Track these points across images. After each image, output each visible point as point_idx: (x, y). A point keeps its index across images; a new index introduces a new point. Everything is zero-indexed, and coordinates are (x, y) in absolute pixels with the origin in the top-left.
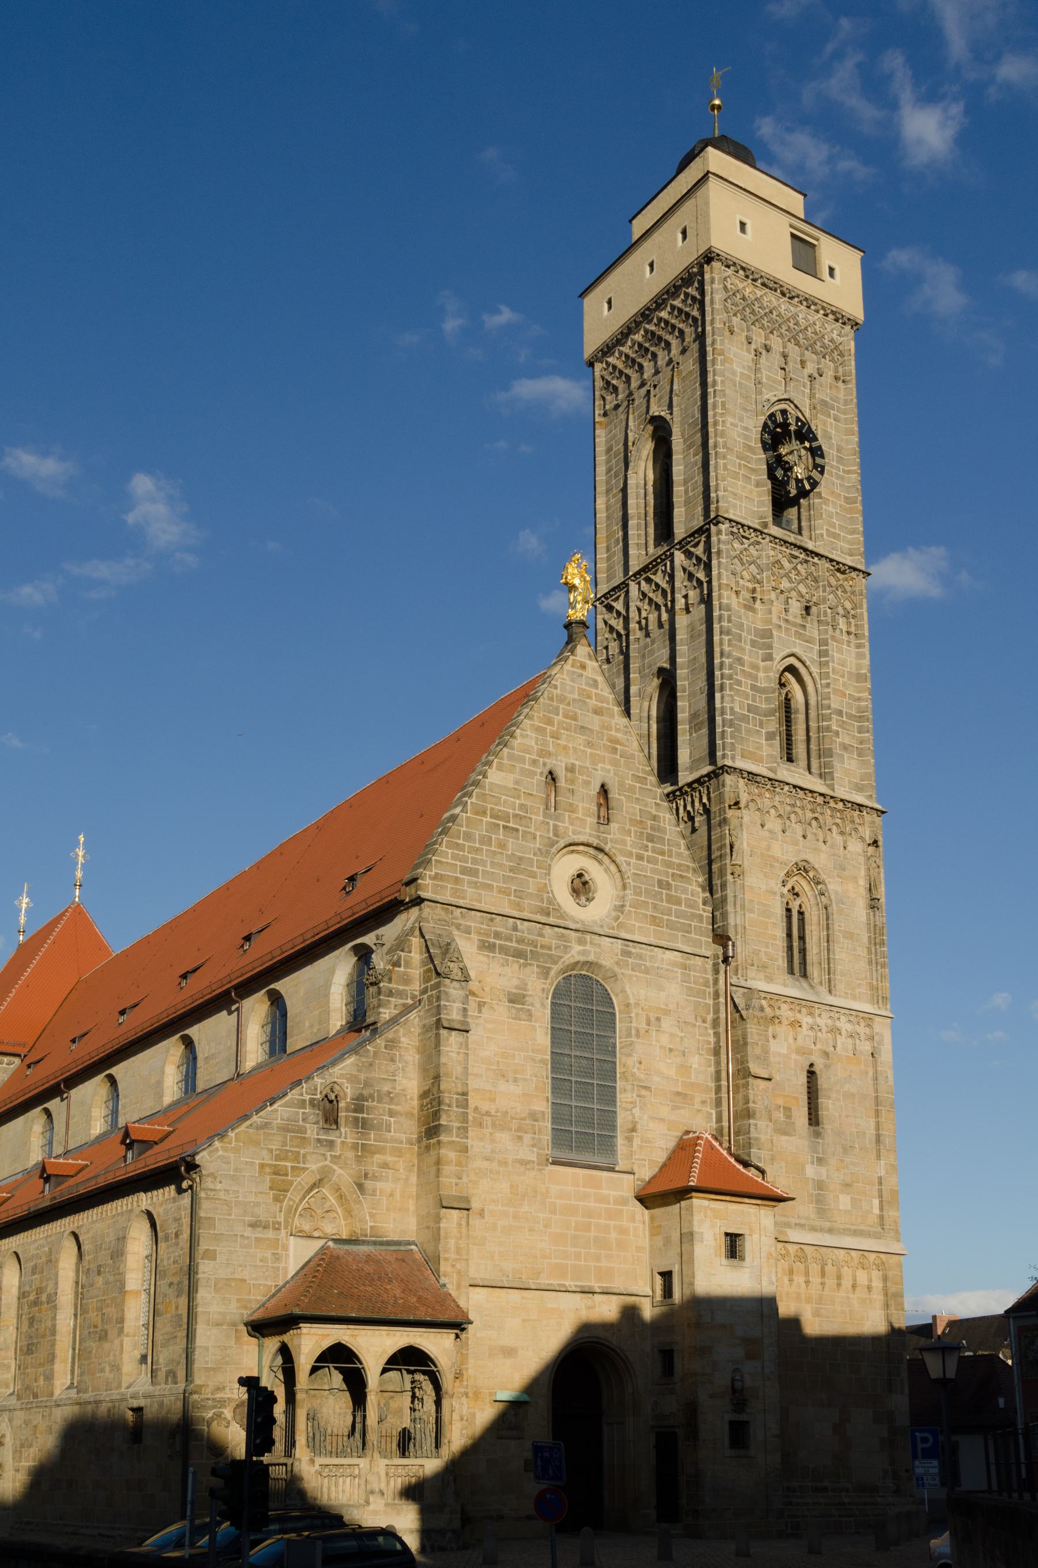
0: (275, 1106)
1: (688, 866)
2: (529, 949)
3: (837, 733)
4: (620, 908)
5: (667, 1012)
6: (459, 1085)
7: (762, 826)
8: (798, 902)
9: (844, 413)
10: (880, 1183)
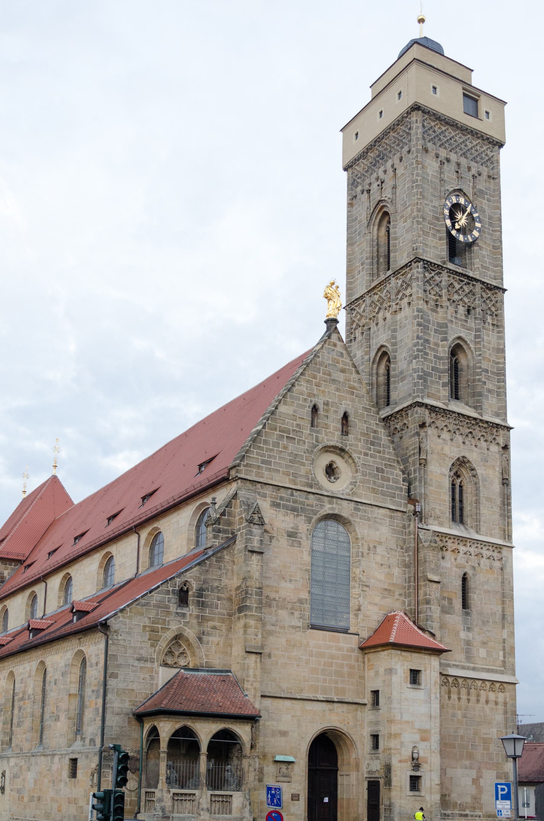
0: (153, 594)
1: (394, 460)
2: (300, 506)
3: (485, 383)
4: (354, 483)
5: (380, 543)
6: (257, 583)
7: (439, 436)
8: (459, 480)
9: (493, 197)
10: (504, 642)
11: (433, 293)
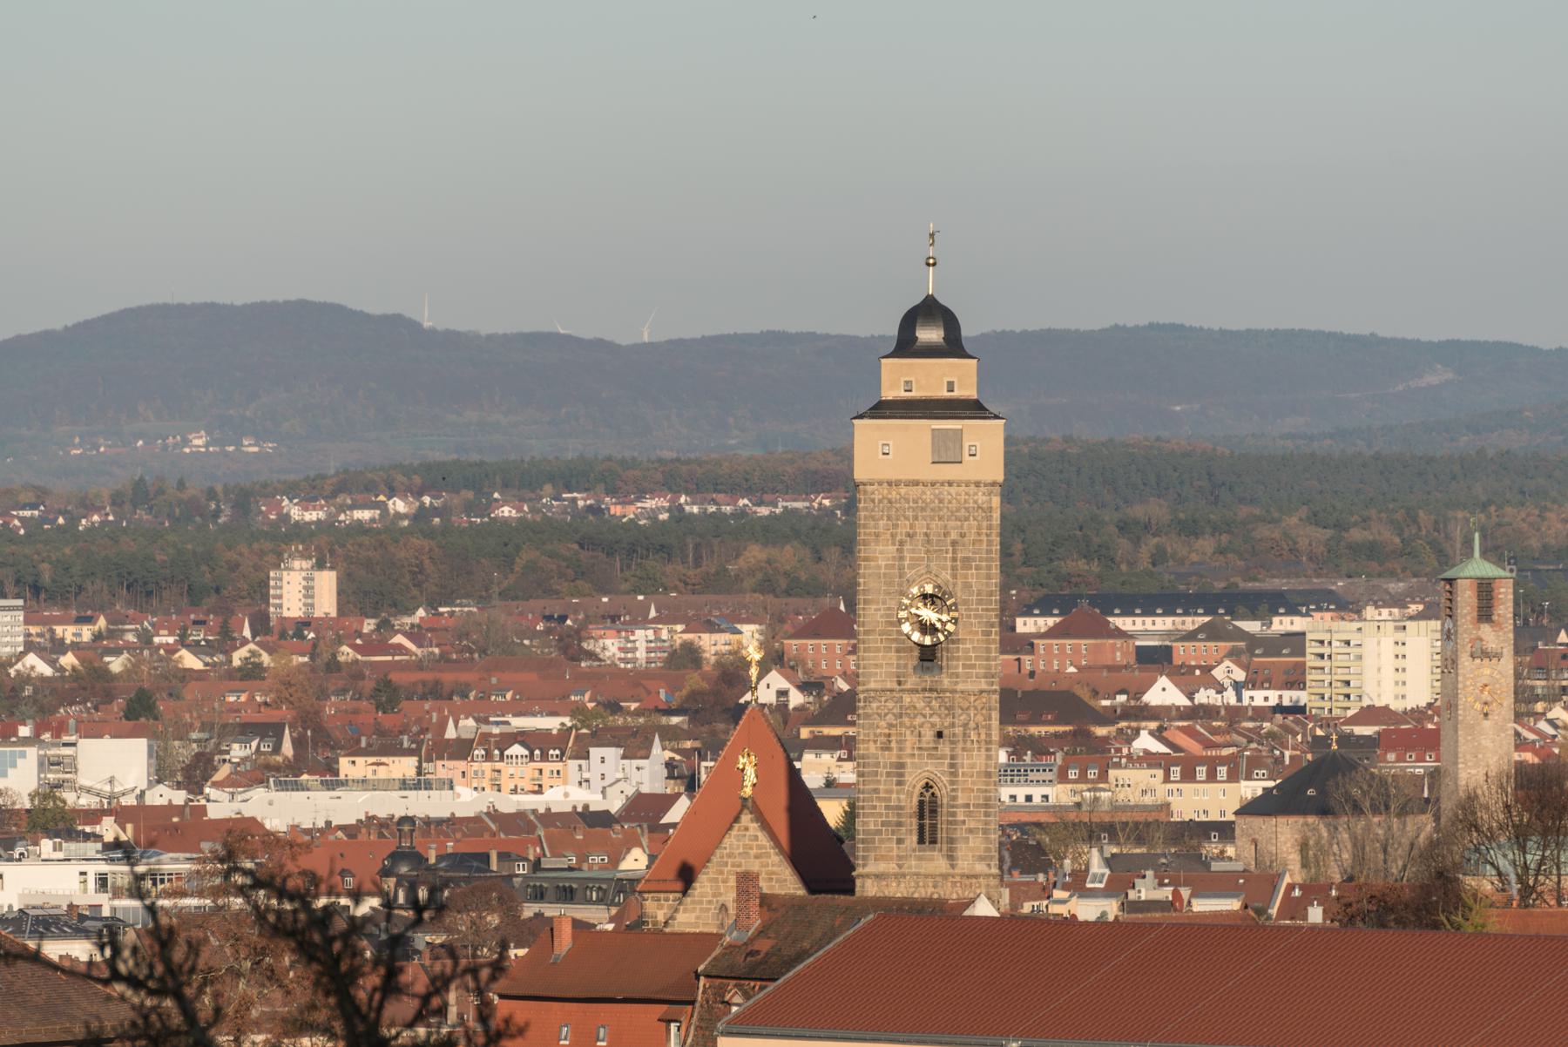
11: (883, 723)
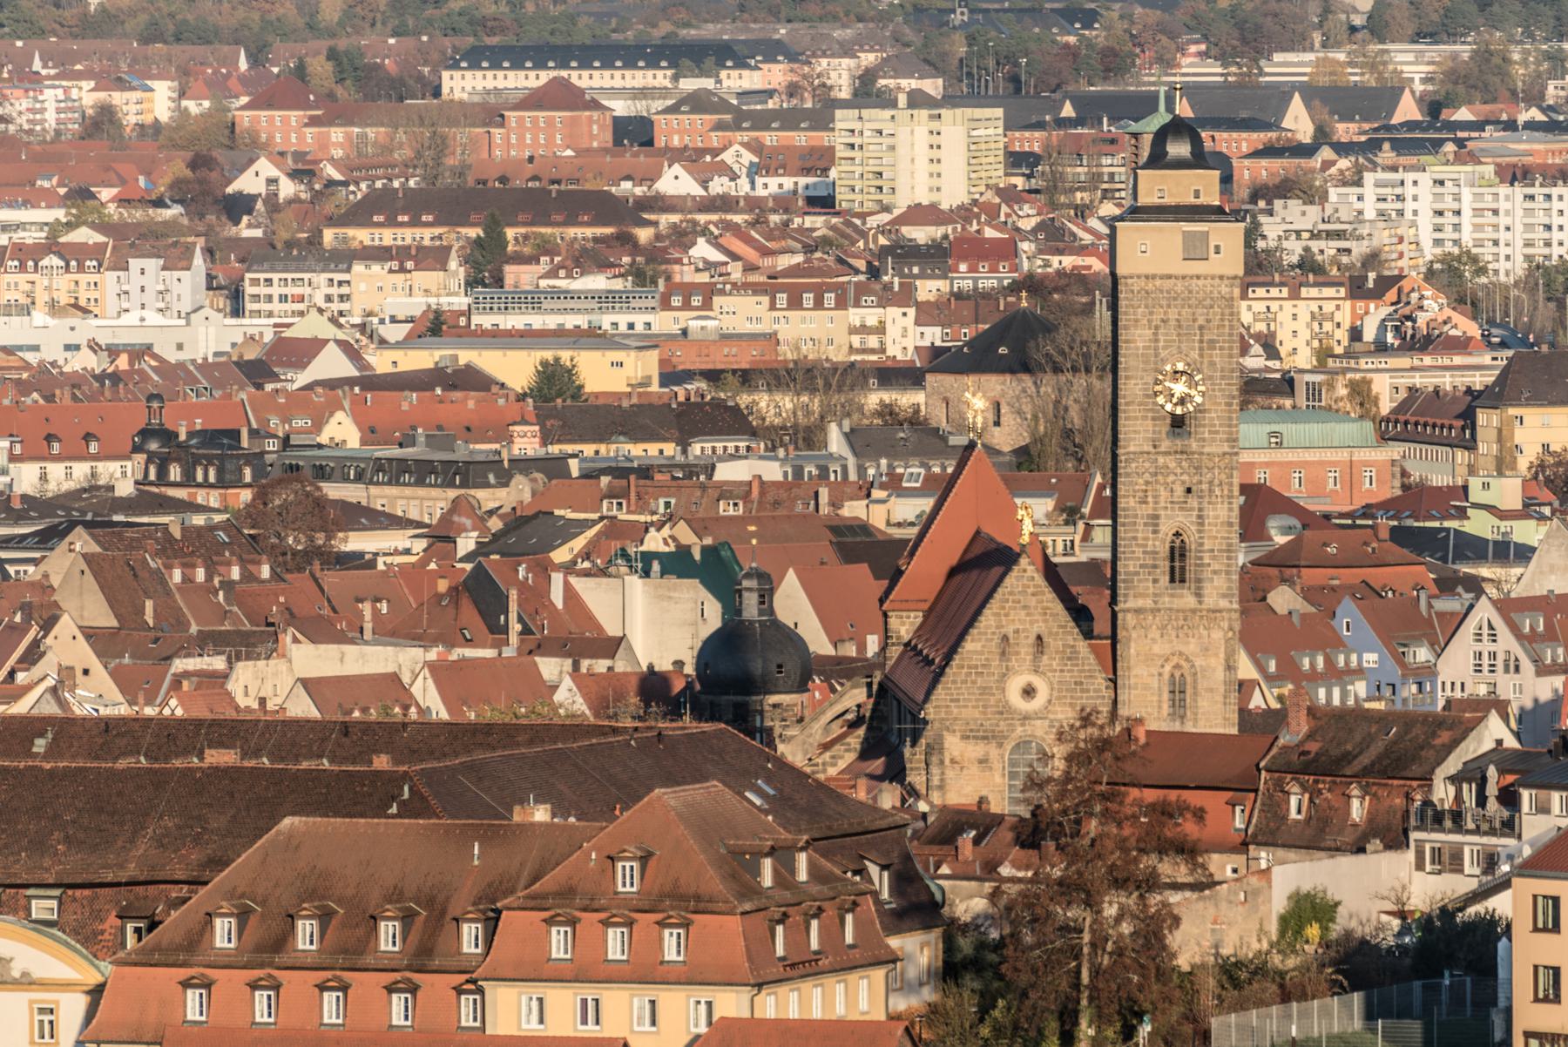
4: (1050, 701)
11: (1141, 481)
